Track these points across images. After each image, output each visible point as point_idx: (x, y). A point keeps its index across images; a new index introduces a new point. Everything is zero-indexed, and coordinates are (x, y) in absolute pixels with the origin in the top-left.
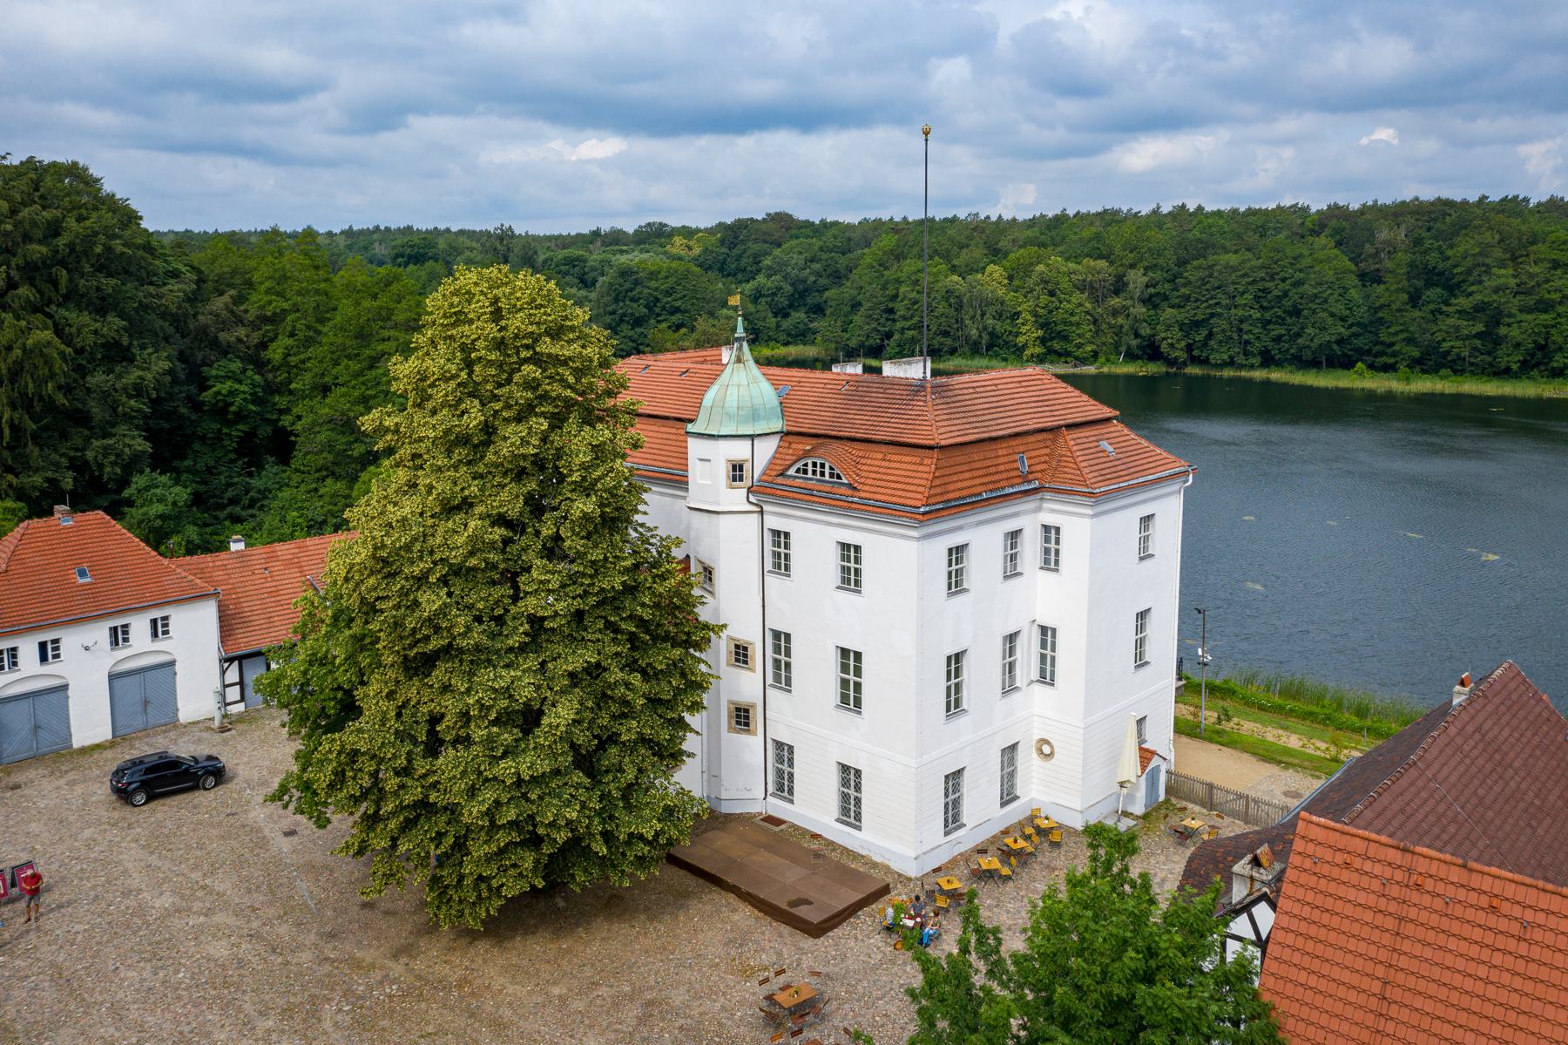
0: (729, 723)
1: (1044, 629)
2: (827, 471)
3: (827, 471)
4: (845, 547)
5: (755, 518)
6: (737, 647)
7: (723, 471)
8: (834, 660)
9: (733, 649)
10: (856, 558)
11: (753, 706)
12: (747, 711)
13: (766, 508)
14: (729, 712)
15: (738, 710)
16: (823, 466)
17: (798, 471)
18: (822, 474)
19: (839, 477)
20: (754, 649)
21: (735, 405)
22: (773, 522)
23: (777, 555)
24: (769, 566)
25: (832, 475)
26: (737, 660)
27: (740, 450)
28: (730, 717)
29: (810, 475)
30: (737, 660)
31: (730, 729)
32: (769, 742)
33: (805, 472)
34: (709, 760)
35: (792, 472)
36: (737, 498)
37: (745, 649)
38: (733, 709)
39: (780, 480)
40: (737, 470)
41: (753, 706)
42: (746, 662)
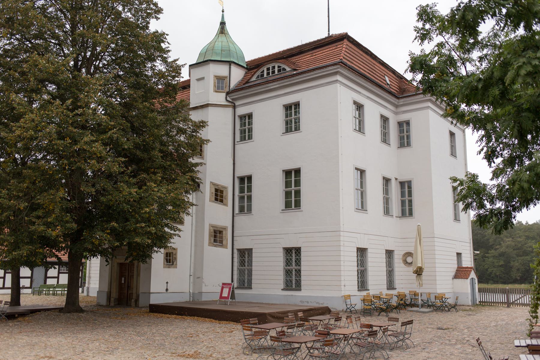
0: (210, 240)
1: (402, 184)
2: (276, 70)
3: (276, 70)
4: (288, 108)
5: (230, 110)
6: (216, 190)
7: (211, 82)
8: (280, 180)
9: (214, 192)
10: (295, 112)
11: (225, 228)
12: (221, 232)
13: (237, 103)
14: (210, 232)
15: (215, 232)
16: (274, 67)
17: (258, 77)
18: (273, 72)
19: (284, 69)
20: (227, 191)
21: (220, 48)
22: (242, 111)
23: (243, 132)
24: (238, 138)
25: (279, 71)
26: (216, 199)
27: (222, 70)
28: (210, 236)
29: (265, 75)
30: (216, 199)
31: (210, 244)
32: (236, 251)
33: (262, 75)
34: (195, 268)
35: (254, 79)
36: (220, 98)
37: (222, 192)
38: (212, 231)
39: (247, 85)
40: (220, 80)
41: (225, 228)
42: (222, 201)
